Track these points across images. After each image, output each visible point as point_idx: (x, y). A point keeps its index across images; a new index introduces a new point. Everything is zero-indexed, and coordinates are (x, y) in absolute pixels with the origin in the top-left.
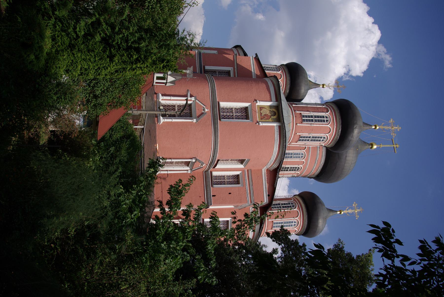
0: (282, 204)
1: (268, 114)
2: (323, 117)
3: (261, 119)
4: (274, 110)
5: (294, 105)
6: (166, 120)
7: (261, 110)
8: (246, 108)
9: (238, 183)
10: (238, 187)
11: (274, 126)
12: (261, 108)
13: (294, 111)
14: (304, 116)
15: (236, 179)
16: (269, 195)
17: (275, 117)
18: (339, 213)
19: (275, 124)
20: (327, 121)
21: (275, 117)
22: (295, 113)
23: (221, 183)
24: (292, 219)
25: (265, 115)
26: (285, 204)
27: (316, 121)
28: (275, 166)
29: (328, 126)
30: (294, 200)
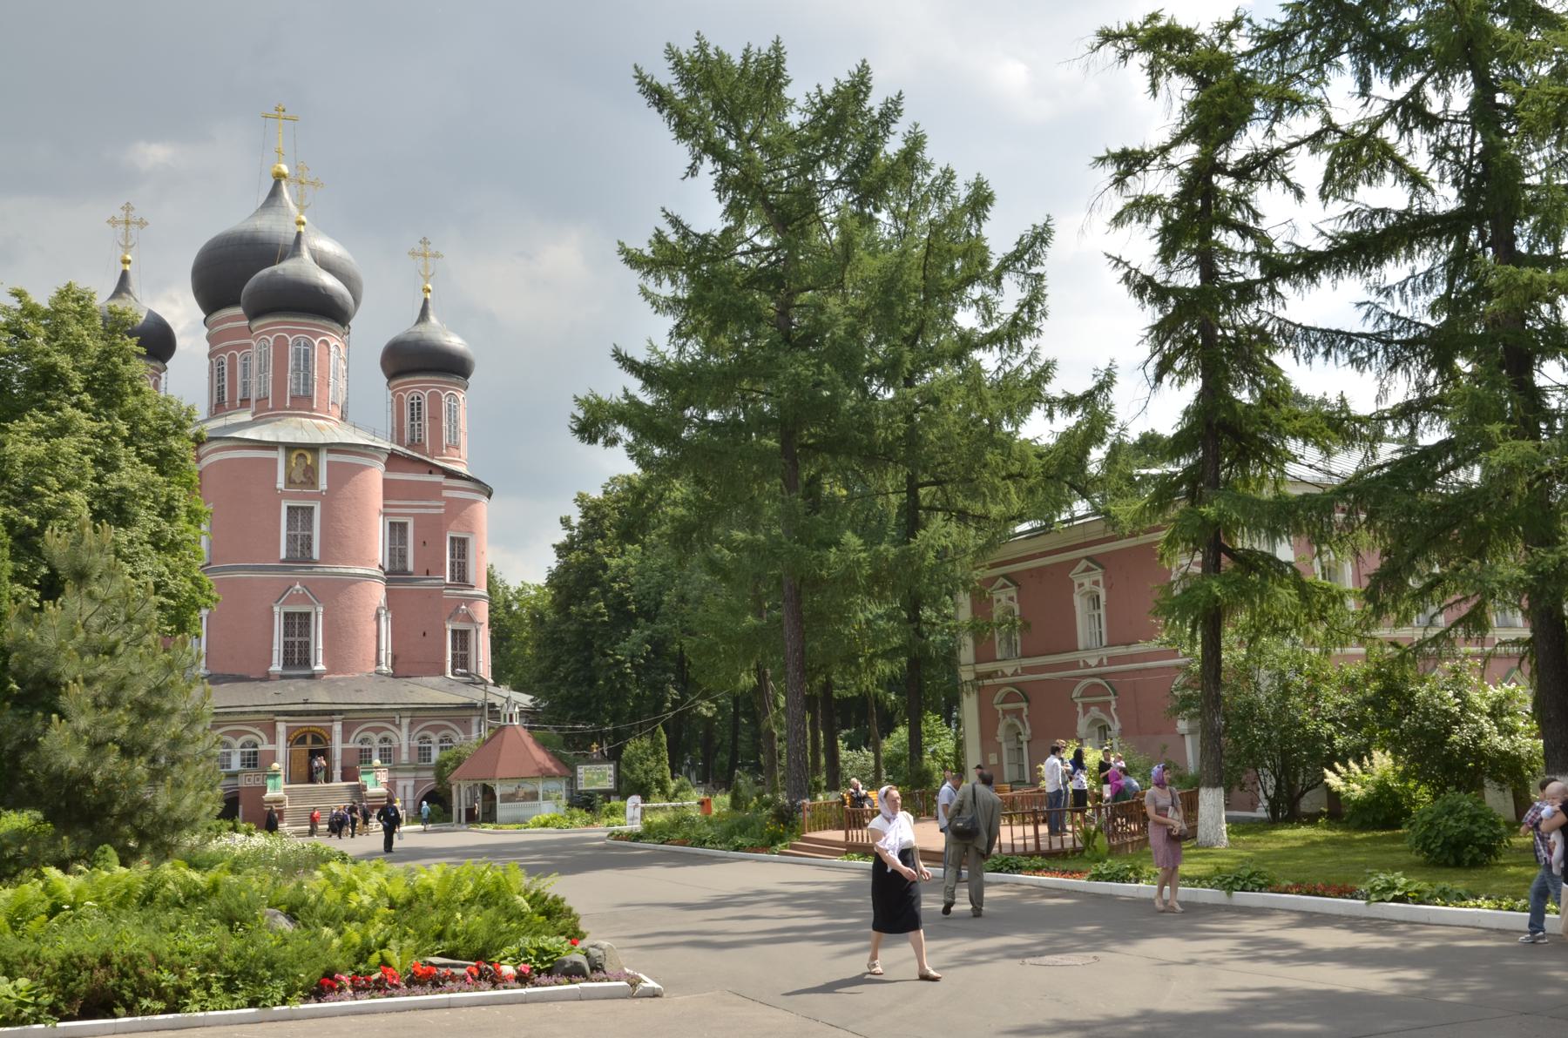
0: (412, 419)
1: (301, 470)
2: (298, 351)
3: (313, 483)
4: (294, 456)
5: (270, 406)
6: (320, 660)
7: (294, 482)
8: (289, 508)
9: (403, 526)
10: (416, 526)
11: (329, 463)
12: (290, 481)
13: (286, 409)
14: (298, 390)
15: (397, 530)
16: (430, 473)
17: (309, 457)
18: (429, 296)
19: (324, 458)
20: (305, 345)
21: (309, 457)
22: (290, 409)
23: (403, 557)
24: (445, 406)
25: (304, 475)
26: (413, 414)
27: (306, 367)
28: (385, 457)
29: (316, 343)
30: (405, 391)
